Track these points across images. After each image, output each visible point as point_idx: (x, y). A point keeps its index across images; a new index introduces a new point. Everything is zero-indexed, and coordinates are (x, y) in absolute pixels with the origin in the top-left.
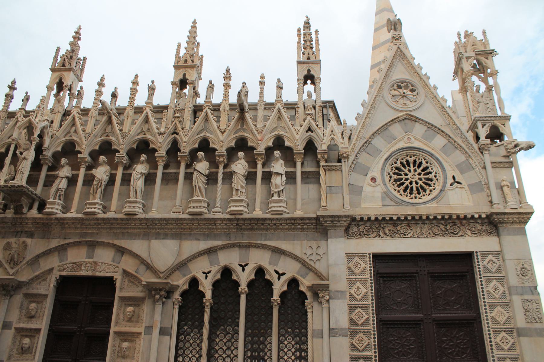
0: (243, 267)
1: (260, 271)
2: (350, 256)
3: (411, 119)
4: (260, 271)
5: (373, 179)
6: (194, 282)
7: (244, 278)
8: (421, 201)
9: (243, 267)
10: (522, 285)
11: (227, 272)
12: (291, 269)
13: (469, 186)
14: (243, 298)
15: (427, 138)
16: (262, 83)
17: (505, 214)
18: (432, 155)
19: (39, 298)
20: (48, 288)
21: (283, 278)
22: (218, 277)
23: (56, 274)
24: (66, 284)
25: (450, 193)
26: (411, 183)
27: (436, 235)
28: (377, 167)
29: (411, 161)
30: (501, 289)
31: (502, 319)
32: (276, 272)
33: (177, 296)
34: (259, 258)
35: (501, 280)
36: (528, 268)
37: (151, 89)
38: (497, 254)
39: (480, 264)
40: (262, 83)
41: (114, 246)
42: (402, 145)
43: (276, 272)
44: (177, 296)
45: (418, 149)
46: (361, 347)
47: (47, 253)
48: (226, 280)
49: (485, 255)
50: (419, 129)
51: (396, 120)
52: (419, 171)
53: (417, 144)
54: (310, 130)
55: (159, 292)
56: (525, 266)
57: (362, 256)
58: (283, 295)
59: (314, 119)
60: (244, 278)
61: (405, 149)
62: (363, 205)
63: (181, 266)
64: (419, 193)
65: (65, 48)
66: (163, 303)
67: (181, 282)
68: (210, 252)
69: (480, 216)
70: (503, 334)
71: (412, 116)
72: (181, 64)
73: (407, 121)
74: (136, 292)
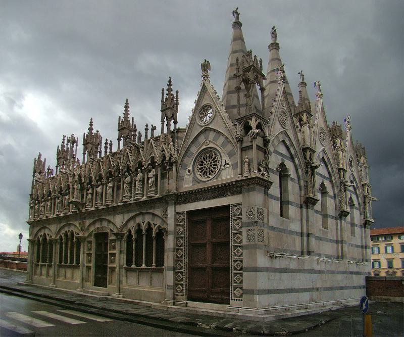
0: (143, 223)
1: (149, 224)
2: (178, 214)
3: (208, 130)
4: (149, 224)
5: (189, 171)
6: (130, 231)
7: (144, 227)
8: (210, 179)
9: (143, 223)
10: (248, 221)
11: (139, 225)
12: (158, 222)
13: (232, 165)
14: (144, 236)
15: (215, 139)
16: (147, 129)
17: (241, 180)
18: (216, 149)
19: (90, 242)
20: (92, 239)
21: (156, 226)
22: (137, 228)
23: (94, 233)
24: (98, 236)
25: (223, 171)
26: (209, 168)
27: (214, 198)
28: (190, 163)
29: (208, 155)
30: (241, 224)
31: (239, 240)
32: (154, 224)
33: (125, 237)
34: (148, 219)
35: (241, 219)
36: (253, 211)
37: (111, 145)
38: (240, 204)
39: (232, 210)
40: (147, 129)
41: (107, 220)
42: (204, 147)
43: (154, 224)
44: (125, 237)
45: (210, 148)
46: (179, 256)
47: (90, 225)
48: (139, 231)
49: (235, 205)
50: (212, 135)
51: (201, 133)
52: (208, 160)
53: (211, 145)
54: (164, 151)
55: (119, 236)
56: (252, 210)
57: (182, 213)
58: (157, 234)
59: (165, 144)
60: (144, 227)
61: (204, 149)
62: (184, 186)
63: (126, 224)
64: (210, 175)
65: (87, 132)
66: (121, 241)
67: (125, 231)
68: (133, 218)
69: (222, 185)
70: (239, 248)
71: (208, 128)
72: (120, 128)
73: (207, 132)
74: (113, 237)
